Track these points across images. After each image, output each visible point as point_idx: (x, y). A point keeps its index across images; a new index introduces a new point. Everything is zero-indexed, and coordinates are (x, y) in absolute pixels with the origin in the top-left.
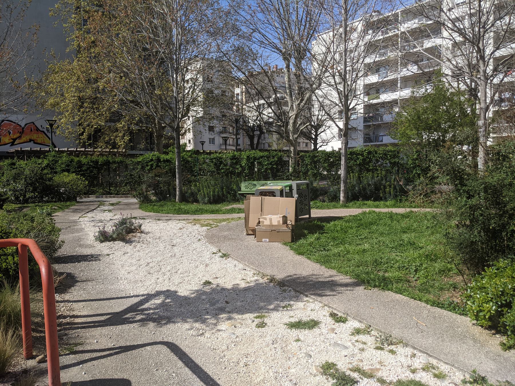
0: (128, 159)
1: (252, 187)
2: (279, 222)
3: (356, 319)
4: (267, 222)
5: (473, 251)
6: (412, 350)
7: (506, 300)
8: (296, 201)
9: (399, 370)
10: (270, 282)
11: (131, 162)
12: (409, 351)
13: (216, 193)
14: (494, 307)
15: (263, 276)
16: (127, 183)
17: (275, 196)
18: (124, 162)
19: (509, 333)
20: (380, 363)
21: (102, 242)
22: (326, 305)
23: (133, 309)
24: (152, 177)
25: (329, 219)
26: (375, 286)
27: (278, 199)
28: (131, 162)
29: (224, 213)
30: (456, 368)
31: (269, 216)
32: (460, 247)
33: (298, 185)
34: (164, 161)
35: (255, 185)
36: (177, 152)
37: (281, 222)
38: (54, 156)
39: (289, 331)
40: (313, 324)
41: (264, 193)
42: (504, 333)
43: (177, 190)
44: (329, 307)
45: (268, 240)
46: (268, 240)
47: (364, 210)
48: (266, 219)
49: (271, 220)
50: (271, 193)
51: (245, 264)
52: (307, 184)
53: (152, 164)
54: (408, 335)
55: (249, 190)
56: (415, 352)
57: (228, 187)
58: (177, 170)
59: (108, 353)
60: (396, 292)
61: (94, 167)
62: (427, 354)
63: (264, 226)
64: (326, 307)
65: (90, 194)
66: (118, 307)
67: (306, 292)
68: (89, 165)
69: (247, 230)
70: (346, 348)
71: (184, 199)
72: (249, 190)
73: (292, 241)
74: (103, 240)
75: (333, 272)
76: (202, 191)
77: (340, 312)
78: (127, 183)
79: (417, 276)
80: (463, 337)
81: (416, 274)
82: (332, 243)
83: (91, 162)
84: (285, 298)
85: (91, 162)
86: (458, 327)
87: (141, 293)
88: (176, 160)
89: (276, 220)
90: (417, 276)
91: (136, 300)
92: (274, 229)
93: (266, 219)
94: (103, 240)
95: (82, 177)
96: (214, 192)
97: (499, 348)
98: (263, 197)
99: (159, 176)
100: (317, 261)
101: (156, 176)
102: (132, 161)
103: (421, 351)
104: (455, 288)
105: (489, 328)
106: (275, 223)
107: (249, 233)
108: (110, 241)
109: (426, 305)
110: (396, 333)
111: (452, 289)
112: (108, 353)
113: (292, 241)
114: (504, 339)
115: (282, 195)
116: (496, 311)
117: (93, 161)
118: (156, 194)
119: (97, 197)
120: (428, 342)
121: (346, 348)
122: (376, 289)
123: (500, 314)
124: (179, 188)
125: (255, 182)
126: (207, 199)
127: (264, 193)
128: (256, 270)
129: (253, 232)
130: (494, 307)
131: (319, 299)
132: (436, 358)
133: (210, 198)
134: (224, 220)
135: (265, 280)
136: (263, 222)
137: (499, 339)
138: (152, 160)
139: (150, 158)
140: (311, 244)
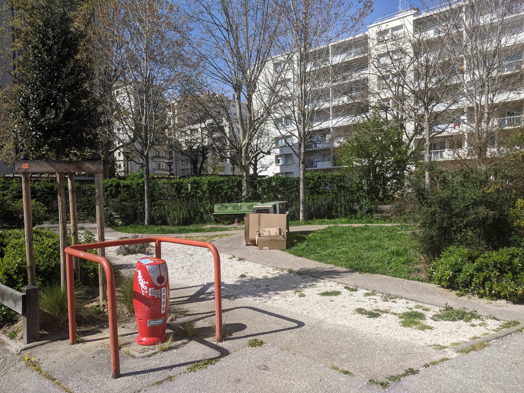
0: (86, 185)
1: (224, 209)
2: (276, 233)
3: (364, 288)
4: (266, 234)
5: (433, 242)
6: (405, 300)
7: (458, 268)
8: (287, 217)
9: (402, 309)
10: (290, 273)
11: (89, 188)
12: (404, 301)
13: (185, 215)
14: (451, 273)
15: (282, 270)
16: (84, 209)
17: (269, 213)
18: (81, 188)
19: (461, 288)
20: (389, 307)
21: (125, 255)
22: (340, 283)
23: (199, 293)
24: (118, 202)
25: (307, 233)
26: (366, 272)
27: (272, 215)
28: (89, 188)
29: (208, 232)
30: (434, 305)
31: (267, 229)
32: (423, 241)
33: (280, 204)
34: (124, 186)
35: (227, 207)
36: (146, 178)
37: (278, 233)
38: (4, 183)
39: (323, 297)
40: (337, 293)
41: (260, 211)
42: (458, 289)
43: (146, 213)
44: (342, 284)
45: (268, 248)
46: (268, 248)
47: (330, 225)
48: (265, 231)
49: (269, 231)
50: (266, 211)
51: (262, 264)
52: (286, 204)
53: (111, 190)
54: (400, 293)
55: (236, 211)
56: (408, 301)
57: (194, 211)
58: (146, 194)
59: (211, 314)
60: (382, 274)
61: (48, 194)
62: (415, 301)
63: (264, 236)
64: (339, 284)
65: (44, 221)
66: (192, 292)
67: (321, 276)
68: (43, 191)
69: (246, 242)
70: (365, 302)
71: (152, 222)
72: (236, 211)
73: (287, 248)
74: (126, 253)
75: (332, 266)
76: (172, 214)
77: (351, 285)
78: (84, 209)
79: (390, 266)
80: (434, 293)
81: (389, 265)
82: (319, 248)
83: (45, 188)
84: (308, 281)
85: (45, 188)
86: (429, 289)
87: (200, 284)
88: (145, 185)
89: (274, 231)
90: (390, 266)
91: (198, 288)
92: (272, 238)
93: (265, 231)
94: (126, 253)
95: (41, 203)
96: (183, 215)
97: (456, 296)
98: (260, 214)
99: (125, 201)
100: (316, 260)
101: (122, 200)
102: (90, 187)
103: (411, 300)
104: (419, 271)
105: (448, 287)
106: (273, 234)
107: (249, 244)
108: (132, 254)
109: (404, 280)
110: (392, 293)
111: (416, 272)
112: (211, 314)
113: (287, 248)
114: (458, 292)
115: (275, 212)
116: (453, 275)
117: (48, 188)
118: (122, 219)
119: (51, 223)
120: (414, 296)
121: (365, 302)
122: (367, 274)
123: (454, 276)
124: (148, 212)
125: (226, 204)
126: (177, 221)
127: (260, 211)
128: (273, 266)
129: (253, 243)
130: (451, 273)
131: (333, 280)
132: (421, 302)
133: (180, 220)
134: (217, 236)
135: (286, 272)
136: (263, 234)
137: (454, 292)
138: (111, 185)
139: (110, 184)
140: (303, 250)
